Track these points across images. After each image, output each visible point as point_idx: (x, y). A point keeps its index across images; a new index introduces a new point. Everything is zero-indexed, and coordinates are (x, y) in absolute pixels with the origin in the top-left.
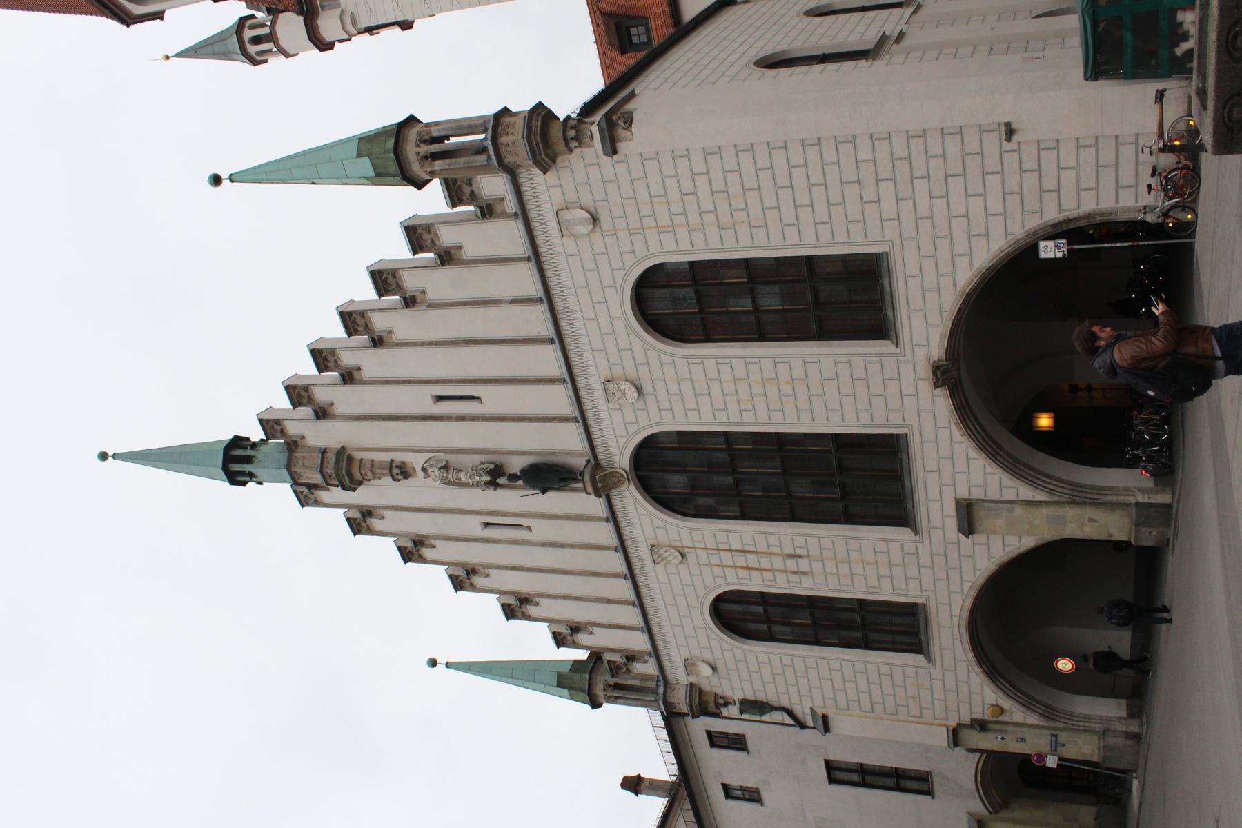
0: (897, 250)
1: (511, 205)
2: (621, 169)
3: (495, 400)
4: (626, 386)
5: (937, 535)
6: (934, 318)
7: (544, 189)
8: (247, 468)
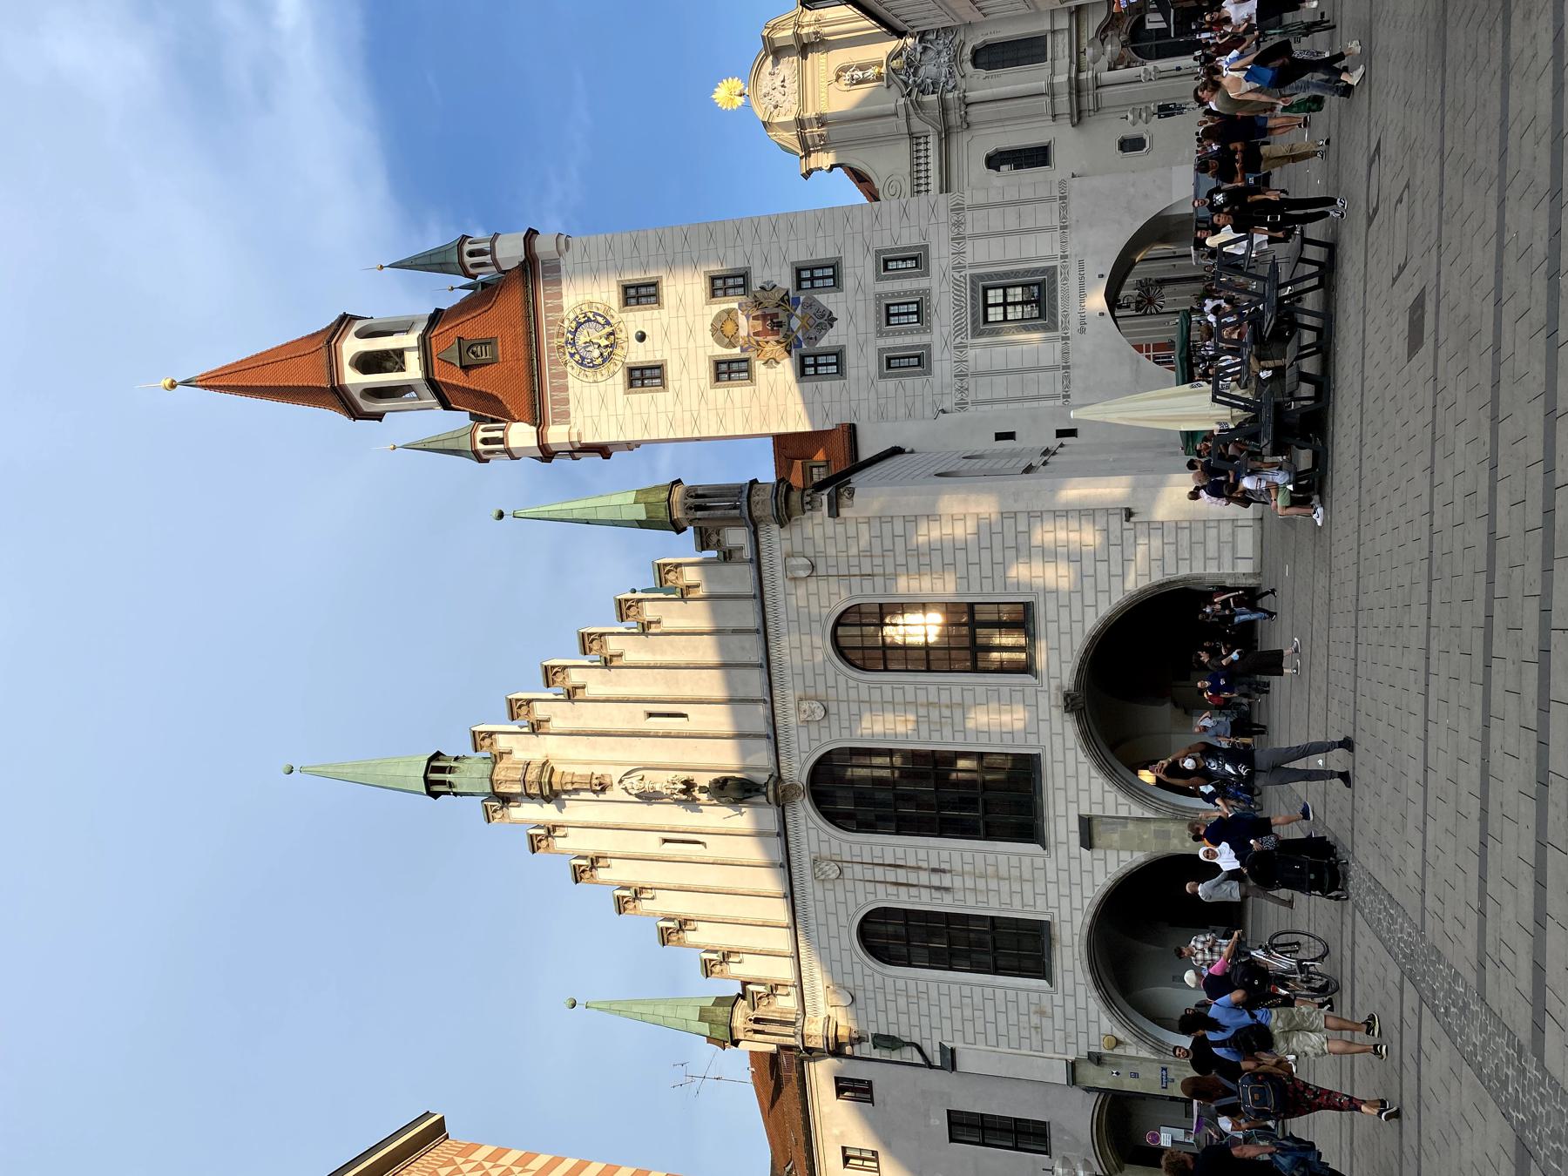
0: (1041, 599)
1: (747, 553)
2: (840, 529)
4: (816, 705)
5: (1062, 850)
6: (1066, 656)
7: (775, 539)
8: (448, 777)
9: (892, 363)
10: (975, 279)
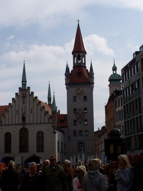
3: (32, 115)
7: (50, 125)
9: (75, 132)
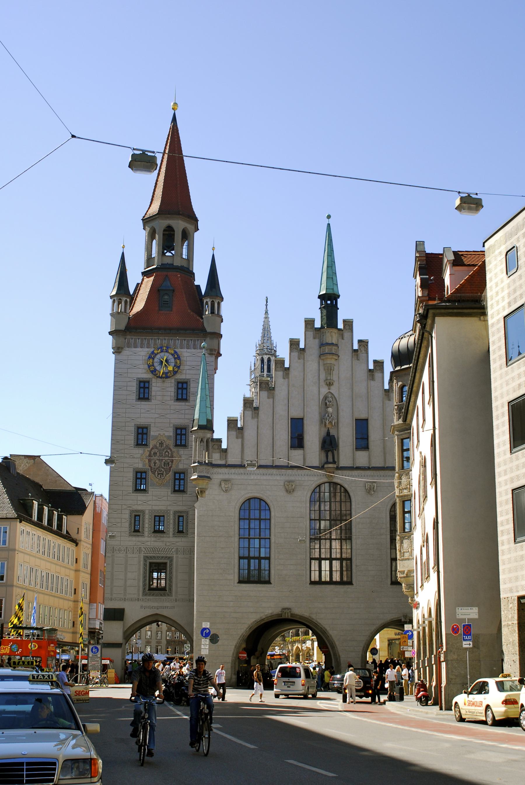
9: (136, 517)
10: (171, 559)
